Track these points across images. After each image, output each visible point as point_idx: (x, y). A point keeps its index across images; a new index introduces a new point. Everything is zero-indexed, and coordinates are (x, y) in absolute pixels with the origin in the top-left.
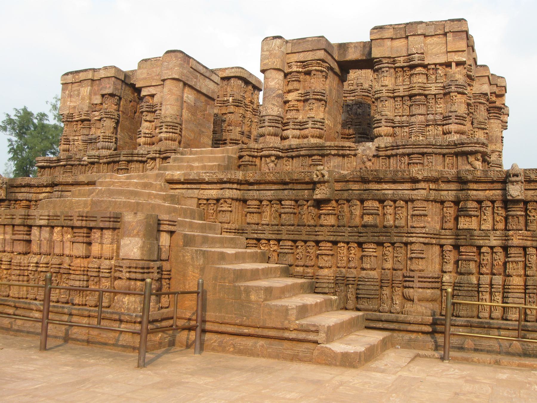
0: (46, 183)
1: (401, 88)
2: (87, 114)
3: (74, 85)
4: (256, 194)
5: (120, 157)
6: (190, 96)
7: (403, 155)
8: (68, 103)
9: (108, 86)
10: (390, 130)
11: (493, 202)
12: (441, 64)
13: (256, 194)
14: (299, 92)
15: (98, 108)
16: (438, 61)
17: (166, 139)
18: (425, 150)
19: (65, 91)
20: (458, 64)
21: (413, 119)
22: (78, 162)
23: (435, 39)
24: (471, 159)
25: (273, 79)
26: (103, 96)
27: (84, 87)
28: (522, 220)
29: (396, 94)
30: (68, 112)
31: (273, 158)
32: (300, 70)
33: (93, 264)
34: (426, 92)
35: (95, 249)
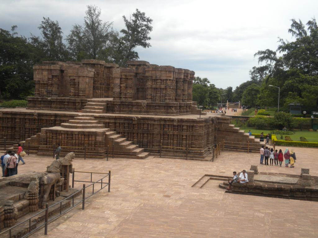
1: (154, 85)
2: (47, 81)
3: (39, 70)
4: (118, 121)
7: (154, 106)
11: (171, 125)
12: (165, 79)
13: (118, 121)
14: (125, 84)
15: (51, 79)
16: (164, 79)
17: (82, 96)
18: (160, 105)
20: (170, 80)
21: (157, 95)
23: (164, 72)
24: (171, 108)
26: (53, 76)
28: (177, 129)
29: (153, 87)
31: (118, 105)
32: (125, 77)
34: (161, 87)
35: (90, 139)
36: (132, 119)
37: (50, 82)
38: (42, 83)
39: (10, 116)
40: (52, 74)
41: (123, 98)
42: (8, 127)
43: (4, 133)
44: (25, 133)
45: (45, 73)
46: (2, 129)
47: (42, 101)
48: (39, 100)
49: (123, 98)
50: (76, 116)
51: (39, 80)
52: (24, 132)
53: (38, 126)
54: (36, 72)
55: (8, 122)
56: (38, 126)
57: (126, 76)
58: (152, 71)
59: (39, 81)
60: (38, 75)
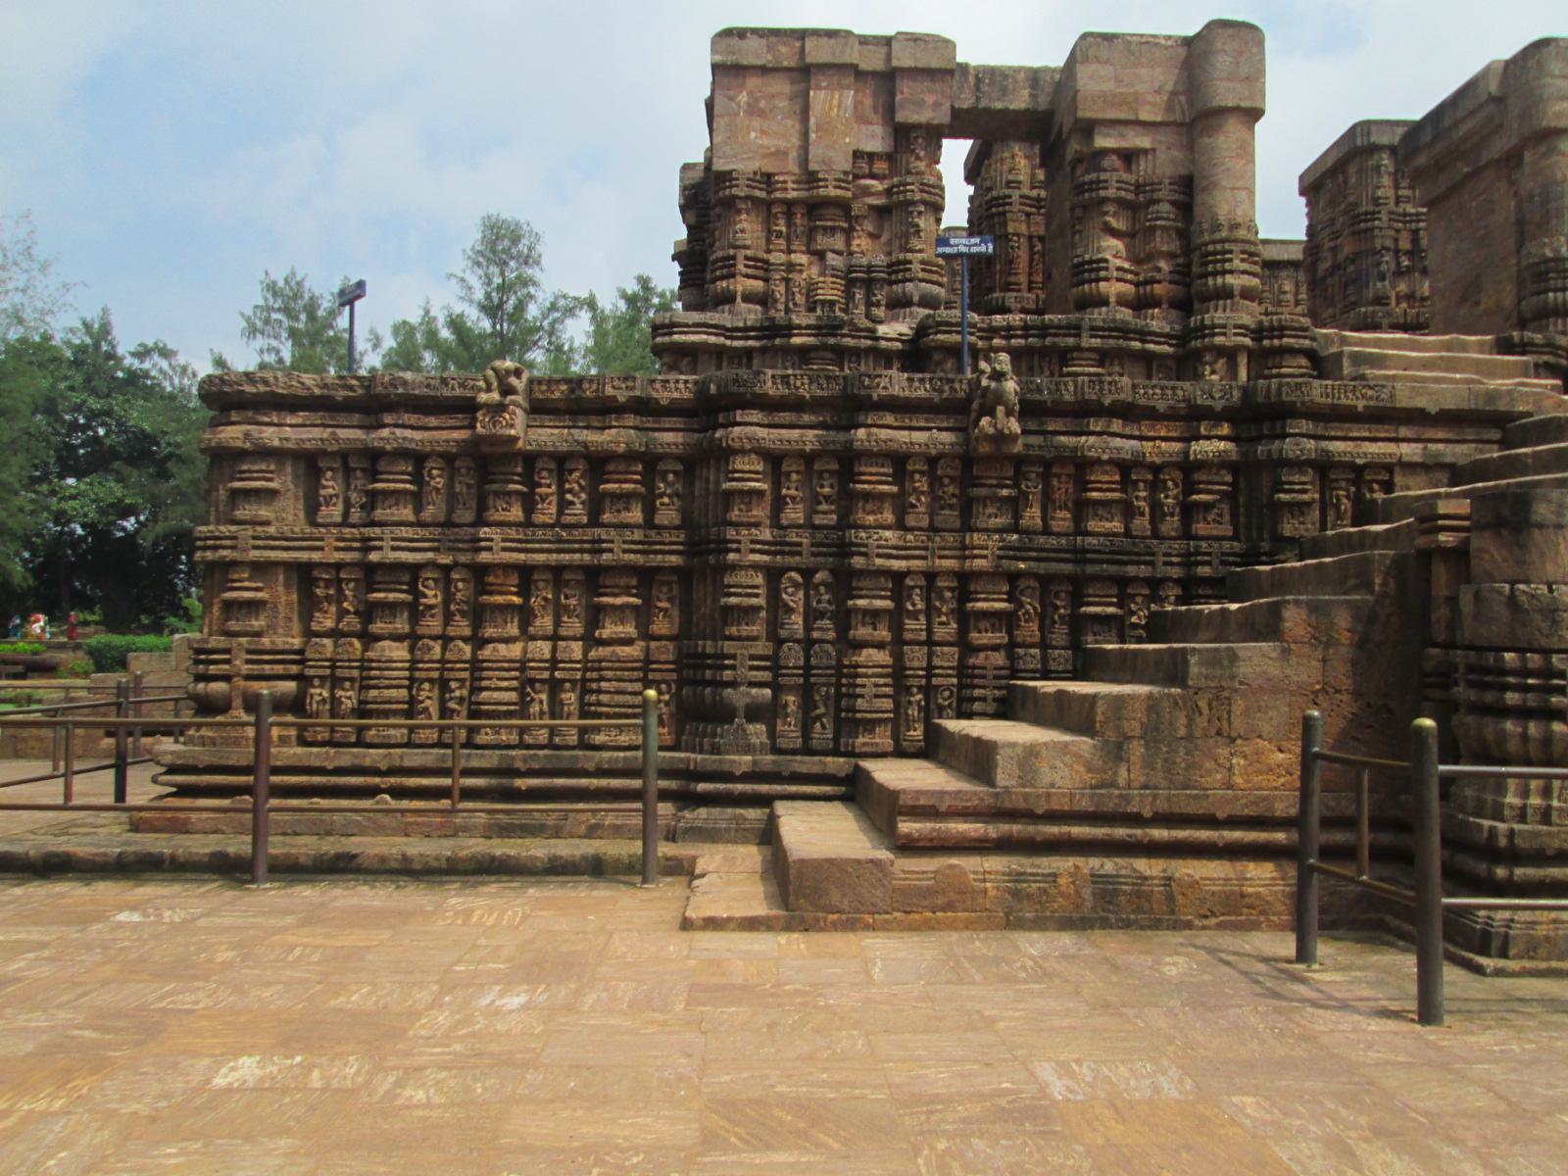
0: (1223, 402)
2: (840, 183)
5: (1078, 336)
8: (753, 135)
9: (930, 99)
19: (731, 93)
22: (869, 342)
27: (825, 88)
30: (755, 165)
37: (867, 192)
38: (789, 204)
39: (616, 437)
40: (901, 117)
42: (594, 578)
43: (543, 648)
44: (849, 645)
46: (516, 600)
47: (824, 347)
48: (796, 340)
51: (769, 167)
52: (826, 629)
53: (1019, 552)
54: (743, 97)
55: (596, 506)
56: (1019, 552)
59: (768, 179)
60: (757, 123)
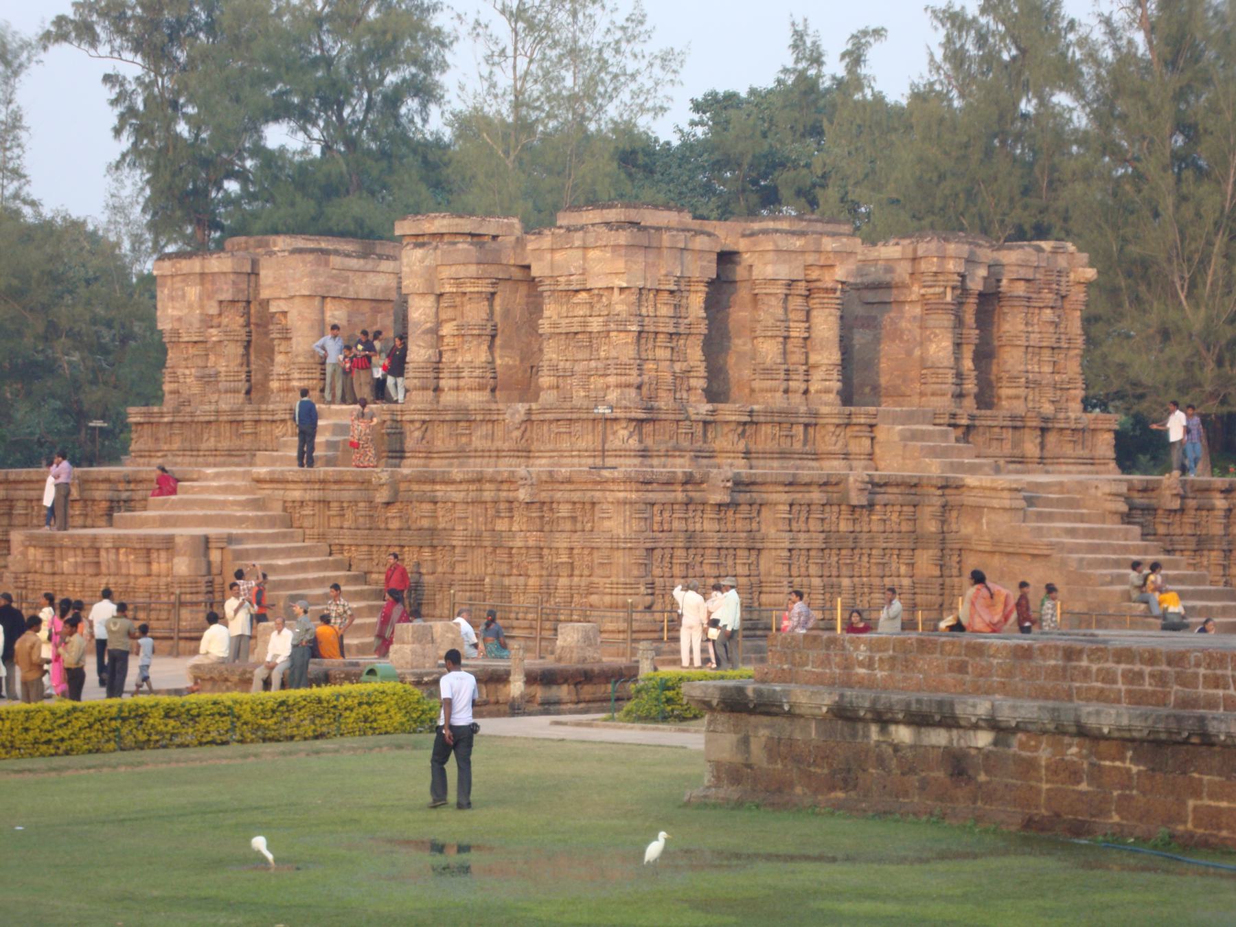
6: (337, 313)
10: (553, 380)
25: (417, 309)
26: (221, 302)
33: (152, 582)
35: (155, 567)
36: (369, 482)
41: (451, 389)
45: (193, 292)
49: (451, 389)
50: (195, 476)
51: (176, 325)
57: (458, 285)
58: (553, 250)
59: (176, 333)
